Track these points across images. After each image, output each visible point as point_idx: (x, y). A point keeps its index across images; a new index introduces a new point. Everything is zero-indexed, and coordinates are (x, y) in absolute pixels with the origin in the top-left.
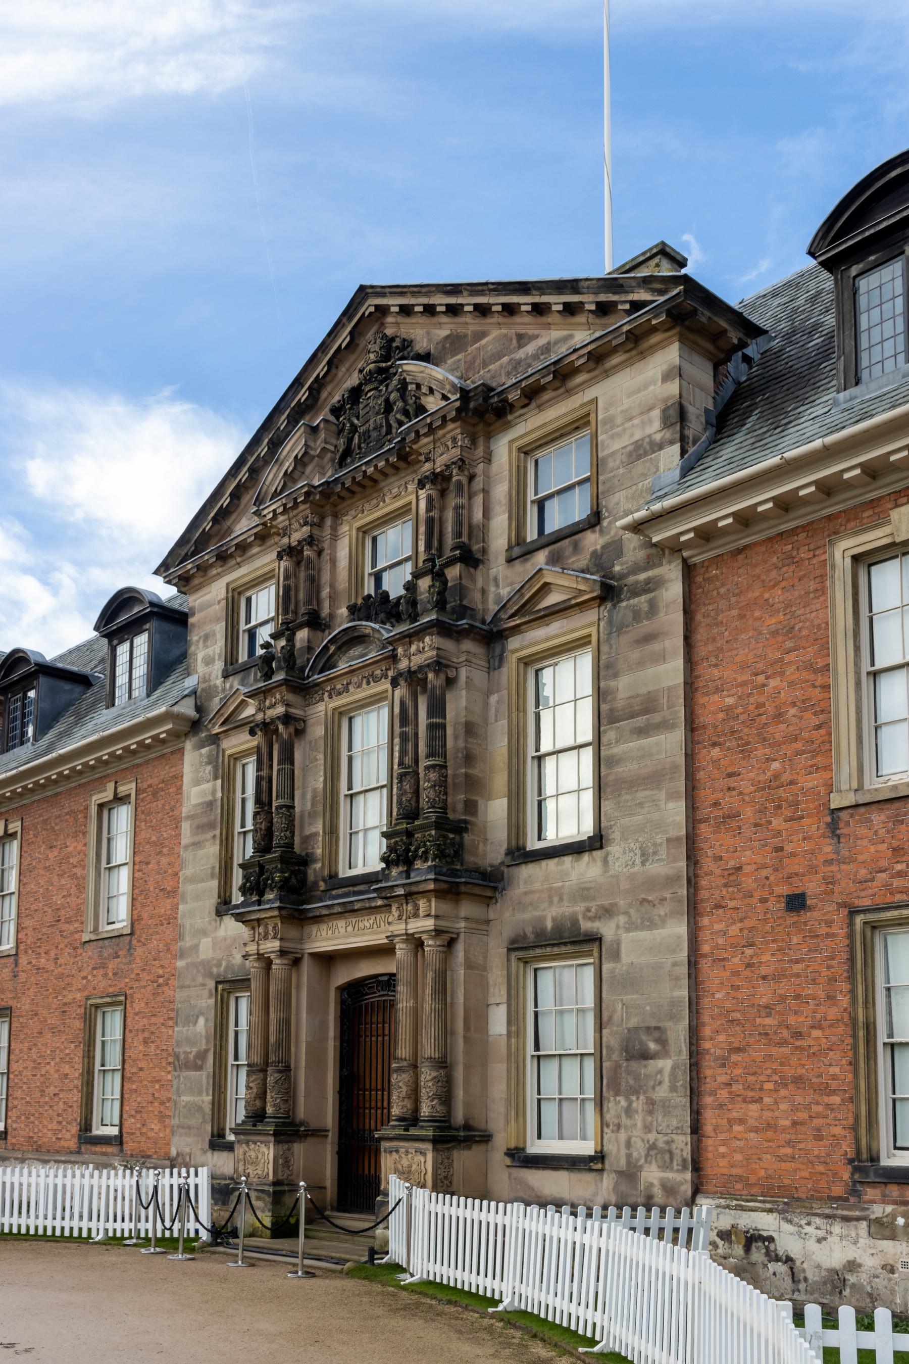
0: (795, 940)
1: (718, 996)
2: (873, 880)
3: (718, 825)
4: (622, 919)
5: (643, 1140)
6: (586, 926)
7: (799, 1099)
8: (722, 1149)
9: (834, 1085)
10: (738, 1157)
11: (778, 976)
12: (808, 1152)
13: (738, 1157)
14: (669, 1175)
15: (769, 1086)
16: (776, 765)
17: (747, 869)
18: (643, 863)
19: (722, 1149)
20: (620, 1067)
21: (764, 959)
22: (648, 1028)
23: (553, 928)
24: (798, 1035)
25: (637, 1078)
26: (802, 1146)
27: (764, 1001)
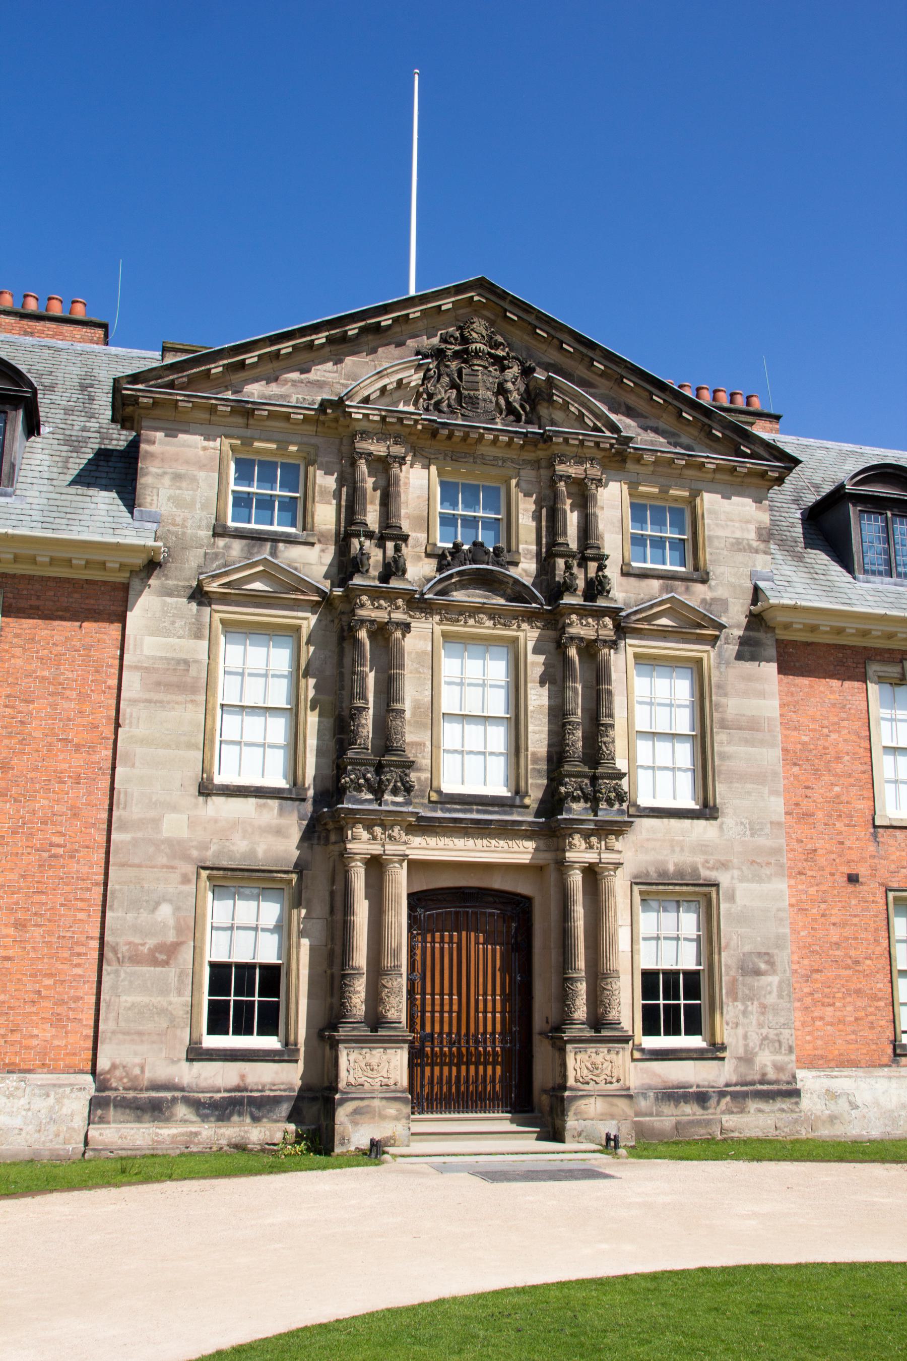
0: (853, 902)
1: (802, 934)
2: (898, 872)
3: (799, 819)
4: (736, 873)
6: (706, 874)
7: (859, 1003)
8: (808, 1038)
9: (880, 994)
10: (819, 1043)
11: (844, 924)
12: (866, 1037)
13: (819, 1043)
15: (839, 995)
16: (837, 789)
17: (820, 852)
18: (752, 835)
19: (808, 1038)
20: (737, 980)
21: (833, 912)
22: (759, 953)
23: (675, 871)
24: (857, 962)
25: (751, 988)
26: (862, 1033)
27: (835, 939)
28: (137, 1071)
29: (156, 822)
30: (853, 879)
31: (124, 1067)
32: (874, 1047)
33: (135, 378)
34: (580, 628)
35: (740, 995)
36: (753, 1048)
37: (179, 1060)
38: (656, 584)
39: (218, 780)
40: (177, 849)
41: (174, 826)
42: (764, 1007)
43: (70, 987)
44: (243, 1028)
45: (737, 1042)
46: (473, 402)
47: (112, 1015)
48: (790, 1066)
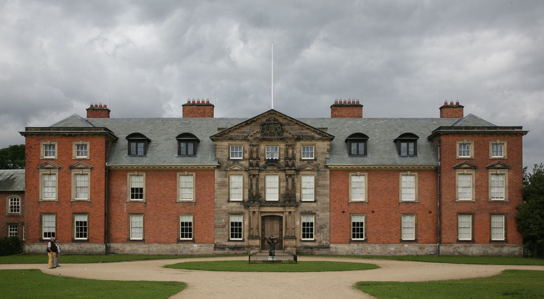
29: (221, 207)
30: (343, 212)
33: (213, 136)
34: (289, 172)
38: (306, 162)
39: (231, 200)
40: (225, 211)
41: (224, 207)
44: (236, 237)
46: (271, 132)
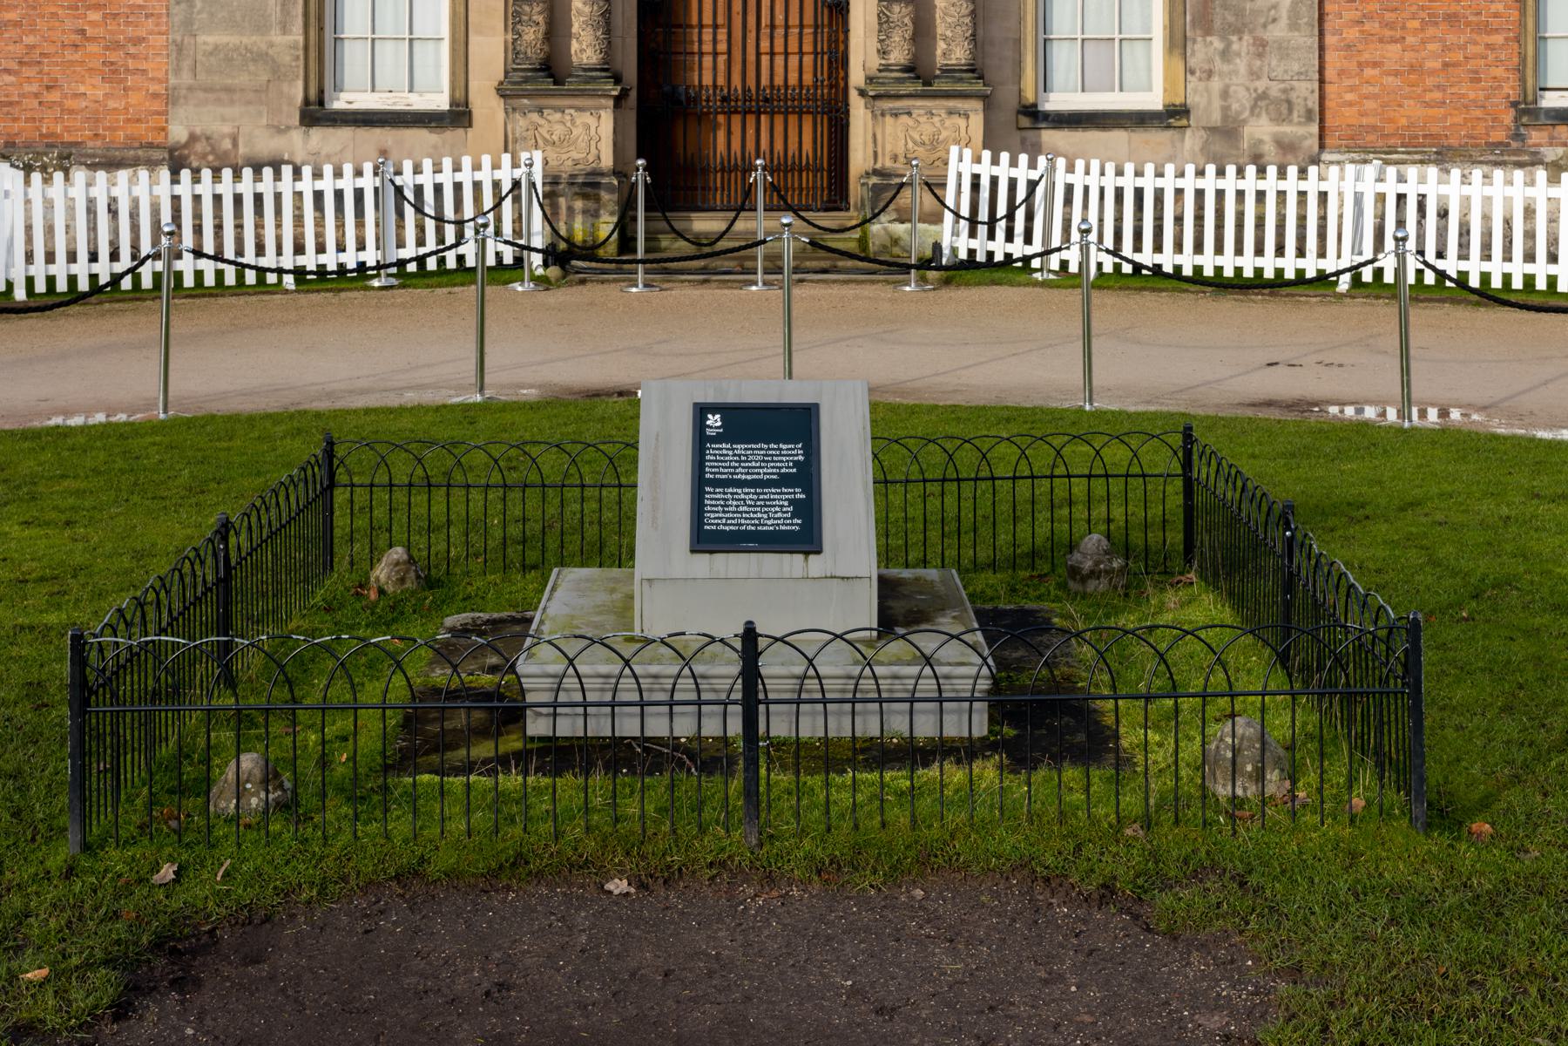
5: (1248, 89)
7: (1451, 38)
8: (1349, 97)
10: (1370, 105)
13: (1370, 105)
14: (1287, 129)
15: (1416, 24)
28: (227, 144)
31: (208, 138)
32: (1478, 113)
35: (1217, 24)
36: (1239, 113)
37: (288, 128)
42: (1261, 46)
43: (128, 24)
45: (1209, 102)
47: (187, 64)
48: (1307, 143)
